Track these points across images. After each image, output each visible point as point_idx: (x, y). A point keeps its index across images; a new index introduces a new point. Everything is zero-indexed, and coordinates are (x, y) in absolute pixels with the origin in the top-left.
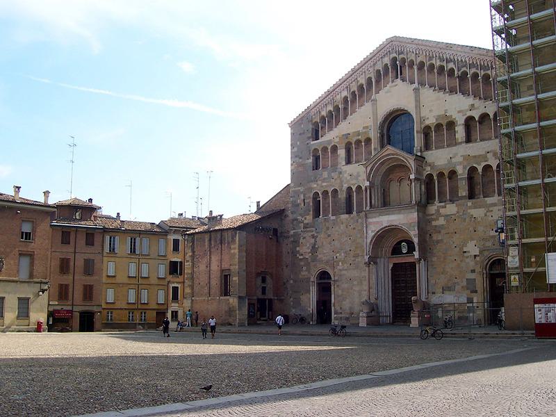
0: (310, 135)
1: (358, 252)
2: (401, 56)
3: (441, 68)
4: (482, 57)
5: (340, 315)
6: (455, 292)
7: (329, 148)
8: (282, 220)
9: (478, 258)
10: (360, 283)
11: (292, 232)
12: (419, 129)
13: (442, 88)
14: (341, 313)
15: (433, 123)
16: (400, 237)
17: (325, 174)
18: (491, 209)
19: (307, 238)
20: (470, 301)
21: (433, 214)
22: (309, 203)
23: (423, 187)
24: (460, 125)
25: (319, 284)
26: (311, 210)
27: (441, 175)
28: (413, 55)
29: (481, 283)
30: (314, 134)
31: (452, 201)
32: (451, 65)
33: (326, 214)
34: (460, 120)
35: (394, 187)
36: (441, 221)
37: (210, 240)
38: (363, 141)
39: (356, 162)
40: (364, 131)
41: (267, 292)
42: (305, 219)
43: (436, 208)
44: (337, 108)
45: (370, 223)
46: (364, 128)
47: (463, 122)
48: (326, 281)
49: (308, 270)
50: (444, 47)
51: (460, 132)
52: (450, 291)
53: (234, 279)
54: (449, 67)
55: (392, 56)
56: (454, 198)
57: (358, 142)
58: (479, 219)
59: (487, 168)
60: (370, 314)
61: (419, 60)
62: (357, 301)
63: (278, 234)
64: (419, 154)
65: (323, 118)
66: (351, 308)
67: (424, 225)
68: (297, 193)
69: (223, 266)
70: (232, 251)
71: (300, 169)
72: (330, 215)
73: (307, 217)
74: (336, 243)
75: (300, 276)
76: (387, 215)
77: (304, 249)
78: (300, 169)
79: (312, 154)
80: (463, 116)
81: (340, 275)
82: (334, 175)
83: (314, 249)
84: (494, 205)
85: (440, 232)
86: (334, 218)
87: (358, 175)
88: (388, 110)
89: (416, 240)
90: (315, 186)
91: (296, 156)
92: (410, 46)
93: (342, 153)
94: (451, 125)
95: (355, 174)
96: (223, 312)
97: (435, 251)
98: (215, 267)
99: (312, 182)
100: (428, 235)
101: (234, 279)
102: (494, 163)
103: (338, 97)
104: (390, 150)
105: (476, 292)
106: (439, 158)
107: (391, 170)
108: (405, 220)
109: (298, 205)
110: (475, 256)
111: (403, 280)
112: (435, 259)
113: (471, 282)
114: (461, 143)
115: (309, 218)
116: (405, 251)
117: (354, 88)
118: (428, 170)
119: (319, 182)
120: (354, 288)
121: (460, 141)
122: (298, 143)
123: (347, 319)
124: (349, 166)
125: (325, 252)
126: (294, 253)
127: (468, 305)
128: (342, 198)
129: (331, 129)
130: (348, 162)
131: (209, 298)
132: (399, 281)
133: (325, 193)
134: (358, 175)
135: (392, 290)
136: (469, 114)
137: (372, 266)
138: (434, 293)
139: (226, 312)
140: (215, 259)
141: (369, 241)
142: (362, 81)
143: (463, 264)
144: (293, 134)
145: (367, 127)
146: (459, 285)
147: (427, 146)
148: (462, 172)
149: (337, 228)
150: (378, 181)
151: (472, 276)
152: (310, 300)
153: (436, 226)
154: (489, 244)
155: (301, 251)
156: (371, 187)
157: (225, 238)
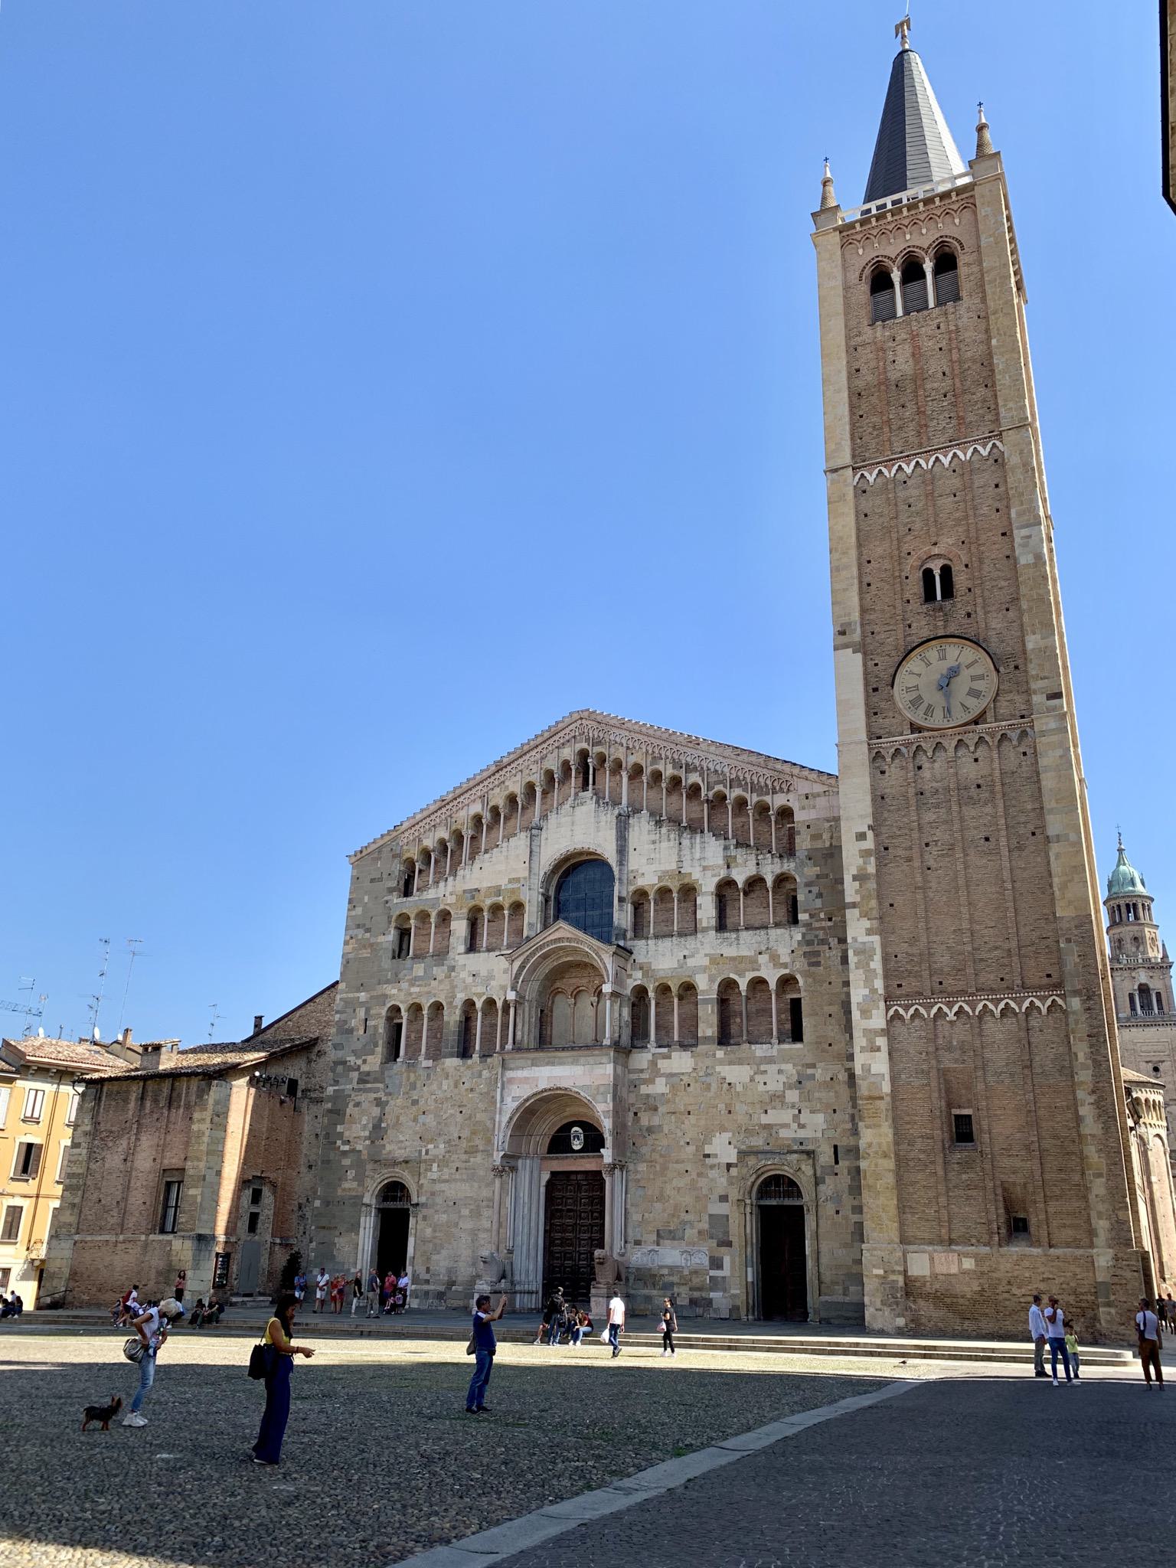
0: (393, 884)
1: (477, 1142)
2: (598, 749)
3: (676, 782)
4: (754, 769)
5: (426, 1287)
6: (683, 1243)
7: (433, 915)
8: (309, 1062)
9: (734, 1171)
10: (476, 1214)
11: (330, 1090)
12: (624, 894)
13: (674, 821)
14: (427, 1282)
16: (569, 1113)
17: (419, 969)
18: (763, 1068)
19: (364, 1106)
20: (716, 1263)
21: (642, 1071)
22: (376, 1027)
23: (626, 1012)
25: (379, 1210)
26: (380, 1042)
27: (664, 989)
28: (622, 750)
29: (742, 1226)
30: (402, 883)
31: (684, 1046)
32: (694, 778)
33: (413, 1053)
34: (708, 885)
35: (562, 1006)
36: (660, 1087)
37: (142, 1098)
38: (506, 905)
39: (489, 950)
40: (510, 886)
41: (259, 1225)
42: (365, 1061)
43: (649, 1056)
44: (459, 837)
45: (511, 1081)
46: (510, 881)
48: (398, 1205)
49: (360, 1179)
50: (684, 742)
52: (674, 1239)
53: (192, 1192)
54: (690, 781)
56: (690, 1041)
57: (496, 909)
58: (739, 1088)
59: (758, 983)
60: (497, 1287)
61: (632, 760)
62: (466, 1253)
63: (299, 1094)
64: (621, 943)
65: (426, 854)
66: (450, 1271)
67: (623, 1091)
68: (351, 1005)
69: (166, 1162)
70: (195, 1127)
71: (366, 953)
72: (421, 1058)
73: (369, 1058)
74: (430, 1120)
75: (340, 1192)
76: (548, 1064)
77: (356, 1131)
78: (366, 953)
79: (393, 924)
80: (714, 876)
81: (433, 1194)
82: (439, 972)
83: (378, 1131)
84: (770, 1060)
85: (656, 1109)
86: (430, 1063)
87: (491, 977)
88: (563, 851)
89: (607, 1125)
90: (394, 991)
91: (358, 926)
92: (617, 731)
93: (460, 927)
94: (689, 892)
95: (484, 973)
96: (153, 1275)
97: (644, 1150)
98: (144, 1162)
99: (388, 982)
100: (631, 1114)
101: (192, 1192)
102: (772, 977)
103: (462, 813)
104: (564, 931)
105: (729, 1244)
106: (662, 958)
107: (561, 971)
108: (585, 1078)
109: (351, 1031)
110: (729, 1166)
111: (569, 1211)
112: (642, 1167)
113: (719, 1222)
114: (705, 930)
115: (374, 1062)
116: (577, 1145)
117: (499, 799)
118: (636, 978)
119: (404, 985)
120: (461, 1225)
121: (704, 924)
122: (366, 899)
123: (440, 1296)
124: (471, 955)
125: (401, 1138)
126: (330, 1138)
127: (713, 1273)
128: (452, 1023)
129: (441, 877)
130: (472, 947)
131: (121, 1238)
132: (561, 1211)
133: (416, 1008)
134: (491, 977)
135: (545, 1231)
136: (723, 873)
137: (509, 1178)
138: (638, 1243)
139: (159, 1273)
140: (147, 1142)
141: (505, 1119)
142: (516, 786)
143: (702, 1183)
144: (356, 879)
145: (518, 880)
146: (692, 1227)
147: (639, 928)
148: (707, 987)
149: (434, 1087)
150: (531, 991)
151: (722, 1209)
152: (360, 1248)
153: (648, 1095)
154: (758, 1142)
155: (347, 1134)
156: (518, 1003)
157: (179, 1096)
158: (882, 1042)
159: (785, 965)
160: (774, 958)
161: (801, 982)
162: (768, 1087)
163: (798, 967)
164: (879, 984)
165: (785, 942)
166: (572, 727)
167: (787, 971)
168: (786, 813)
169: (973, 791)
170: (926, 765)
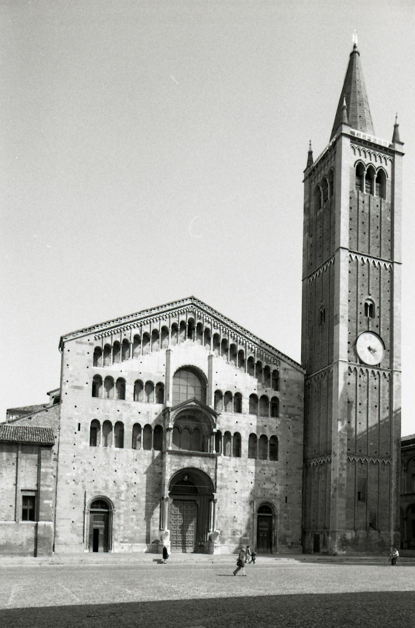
3: (233, 347)
15: (224, 390)
18: (264, 468)
24: (246, 398)
47: (248, 397)
51: (246, 404)
55: (190, 316)
94: (239, 396)
102: (269, 435)
158: (345, 467)
159: (273, 432)
160: (270, 428)
161: (279, 439)
162: (267, 475)
163: (279, 434)
164: (346, 448)
165: (273, 422)
166: (186, 307)
167: (274, 434)
168: (276, 372)
169: (374, 390)
170: (362, 376)
